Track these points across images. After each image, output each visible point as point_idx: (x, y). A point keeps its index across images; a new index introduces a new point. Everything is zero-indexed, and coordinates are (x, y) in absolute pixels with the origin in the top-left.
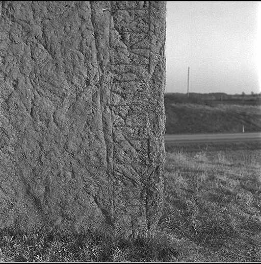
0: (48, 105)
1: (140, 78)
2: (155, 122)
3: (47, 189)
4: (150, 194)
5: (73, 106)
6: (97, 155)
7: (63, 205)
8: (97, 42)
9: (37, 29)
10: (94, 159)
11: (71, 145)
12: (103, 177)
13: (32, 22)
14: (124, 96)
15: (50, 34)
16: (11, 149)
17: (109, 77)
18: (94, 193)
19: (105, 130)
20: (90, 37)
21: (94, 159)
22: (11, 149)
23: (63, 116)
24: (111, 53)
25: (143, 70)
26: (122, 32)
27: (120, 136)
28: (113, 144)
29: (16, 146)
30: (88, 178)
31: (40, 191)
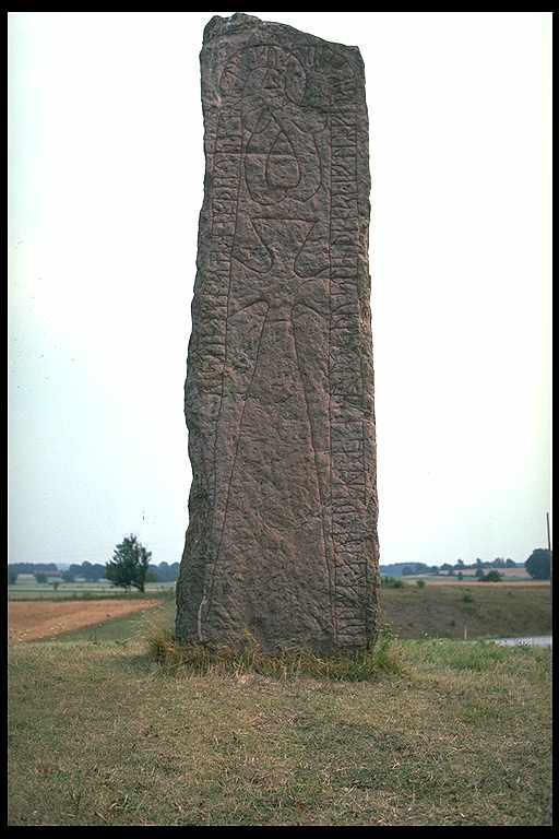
0: (276, 535)
6: (321, 580)
8: (320, 479)
13: (263, 462)
18: (318, 613)
23: (290, 545)
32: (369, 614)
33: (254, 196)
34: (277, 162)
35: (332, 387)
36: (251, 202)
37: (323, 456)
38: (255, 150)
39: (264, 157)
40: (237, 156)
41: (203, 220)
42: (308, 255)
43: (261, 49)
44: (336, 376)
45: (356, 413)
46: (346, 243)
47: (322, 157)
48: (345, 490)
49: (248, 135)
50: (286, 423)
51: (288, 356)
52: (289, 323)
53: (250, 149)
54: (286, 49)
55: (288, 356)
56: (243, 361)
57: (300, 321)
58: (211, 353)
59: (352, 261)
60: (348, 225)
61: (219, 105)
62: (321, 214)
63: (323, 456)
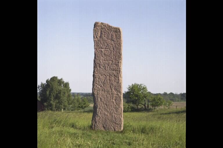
0: (106, 113)
1: (119, 110)
2: (121, 116)
3: (106, 126)
4: (121, 126)
5: (110, 113)
7: (108, 128)
9: (105, 103)
10: (113, 121)
11: (110, 119)
12: (114, 124)
14: (117, 112)
15: (107, 103)
16: (101, 120)
17: (115, 109)
19: (114, 117)
20: (112, 104)
21: (113, 121)
22: (101, 120)
23: (109, 115)
24: (115, 106)
25: (119, 108)
26: (116, 103)
28: (115, 119)
29: (102, 119)
30: (112, 124)
31: (105, 126)
33: (102, 56)
34: (106, 50)
35: (115, 89)
36: (102, 58)
37: (114, 101)
38: (103, 48)
39: (104, 50)
40: (100, 49)
42: (111, 67)
45: (119, 93)
46: (117, 65)
47: (114, 50)
49: (101, 46)
51: (108, 84)
53: (102, 48)
54: (108, 29)
55: (108, 84)
56: (101, 85)
57: (110, 79)
58: (96, 84)
61: (96, 40)
62: (114, 60)
63: (114, 101)
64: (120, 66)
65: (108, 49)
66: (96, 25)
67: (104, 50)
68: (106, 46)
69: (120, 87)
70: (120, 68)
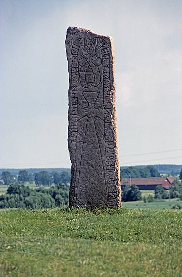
23: (96, 182)
27: (109, 186)
32: (117, 200)
34: (88, 75)
36: (82, 87)
39: (85, 73)
41: (69, 93)
43: (82, 39)
44: (106, 136)
45: (112, 146)
48: (109, 167)
50: (94, 150)
51: (94, 131)
52: (93, 122)
57: (96, 122)
59: (109, 104)
60: (108, 93)
64: (113, 101)
65: (91, 72)
66: (71, 32)
67: (85, 73)
68: (88, 68)
69: (113, 136)
70: (112, 105)
